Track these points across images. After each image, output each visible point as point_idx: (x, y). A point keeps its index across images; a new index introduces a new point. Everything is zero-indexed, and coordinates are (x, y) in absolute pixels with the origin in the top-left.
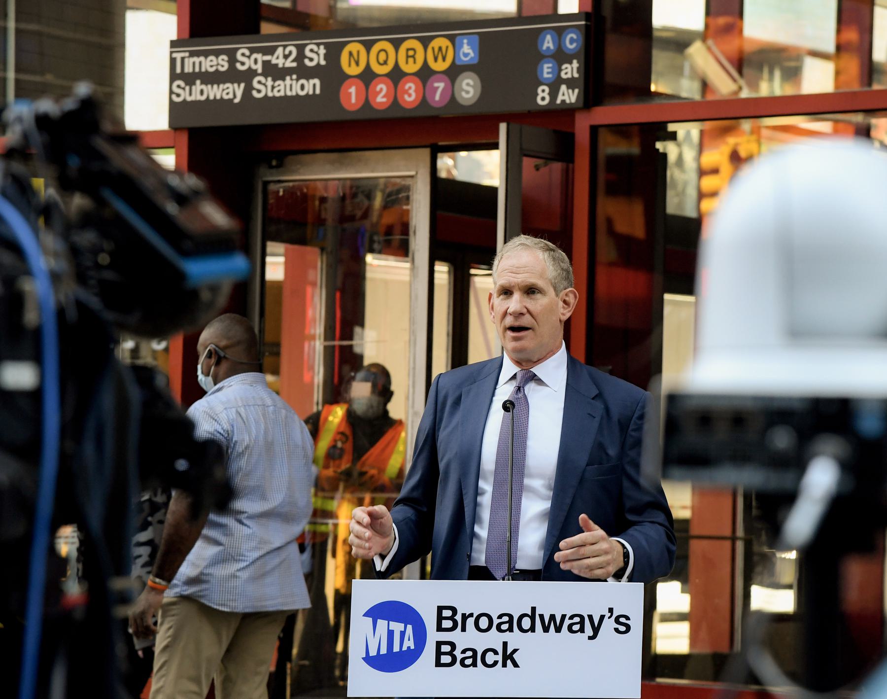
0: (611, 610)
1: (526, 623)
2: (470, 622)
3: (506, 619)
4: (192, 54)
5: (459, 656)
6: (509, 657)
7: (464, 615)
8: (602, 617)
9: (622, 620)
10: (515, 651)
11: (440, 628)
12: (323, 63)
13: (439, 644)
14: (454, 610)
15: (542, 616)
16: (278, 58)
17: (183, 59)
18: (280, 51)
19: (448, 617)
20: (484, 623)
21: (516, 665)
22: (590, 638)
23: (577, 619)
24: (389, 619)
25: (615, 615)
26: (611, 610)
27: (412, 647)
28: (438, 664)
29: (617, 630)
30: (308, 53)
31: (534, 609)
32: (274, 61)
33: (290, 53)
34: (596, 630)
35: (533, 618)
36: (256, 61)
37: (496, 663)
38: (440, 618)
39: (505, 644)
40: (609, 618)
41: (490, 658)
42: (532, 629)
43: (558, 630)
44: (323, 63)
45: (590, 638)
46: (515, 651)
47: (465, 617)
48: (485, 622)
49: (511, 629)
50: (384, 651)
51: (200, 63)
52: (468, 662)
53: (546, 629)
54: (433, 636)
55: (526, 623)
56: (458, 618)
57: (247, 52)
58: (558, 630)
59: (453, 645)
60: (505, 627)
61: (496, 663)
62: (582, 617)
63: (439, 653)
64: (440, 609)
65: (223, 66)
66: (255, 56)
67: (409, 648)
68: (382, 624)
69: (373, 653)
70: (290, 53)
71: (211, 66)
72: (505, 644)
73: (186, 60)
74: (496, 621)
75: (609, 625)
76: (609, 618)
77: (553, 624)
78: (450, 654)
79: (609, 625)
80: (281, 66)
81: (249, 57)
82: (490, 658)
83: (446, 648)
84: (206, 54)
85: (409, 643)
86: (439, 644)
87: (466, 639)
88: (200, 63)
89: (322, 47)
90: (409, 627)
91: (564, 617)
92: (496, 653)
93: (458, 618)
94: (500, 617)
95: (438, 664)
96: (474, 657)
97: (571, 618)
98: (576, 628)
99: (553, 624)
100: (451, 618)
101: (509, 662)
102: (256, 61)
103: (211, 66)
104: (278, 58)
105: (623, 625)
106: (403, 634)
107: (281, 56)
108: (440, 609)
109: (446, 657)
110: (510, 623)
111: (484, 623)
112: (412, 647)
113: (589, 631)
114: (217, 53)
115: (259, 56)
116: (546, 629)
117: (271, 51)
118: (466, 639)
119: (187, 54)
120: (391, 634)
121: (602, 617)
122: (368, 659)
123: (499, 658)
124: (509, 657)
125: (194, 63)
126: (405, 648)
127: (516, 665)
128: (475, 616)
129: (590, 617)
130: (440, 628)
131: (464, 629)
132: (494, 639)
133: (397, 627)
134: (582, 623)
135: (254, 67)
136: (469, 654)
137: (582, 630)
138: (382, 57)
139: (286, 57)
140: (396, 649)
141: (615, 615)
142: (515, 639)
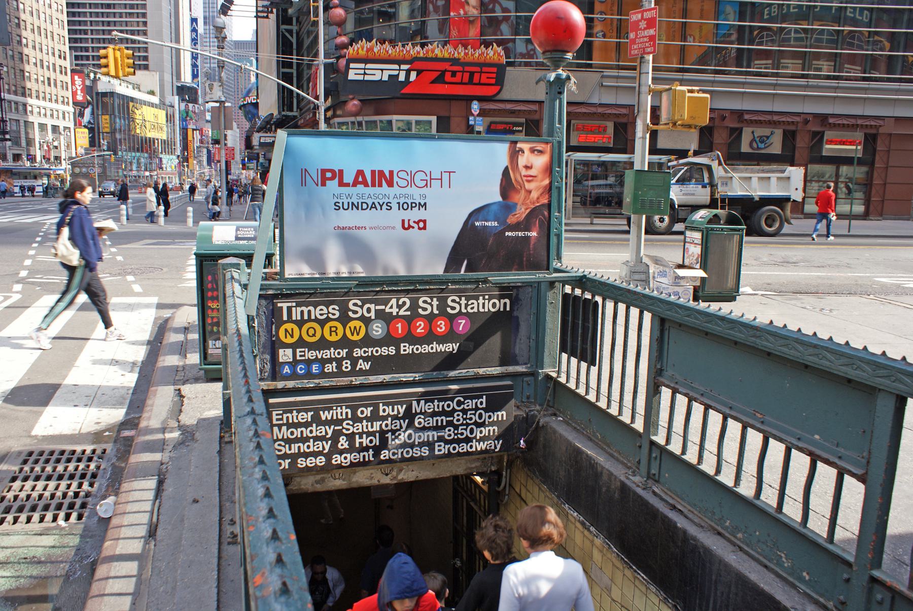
4: (299, 305)
16: (391, 307)
17: (289, 309)
18: (394, 301)
32: (388, 310)
33: (404, 303)
36: (369, 310)
51: (309, 312)
57: (360, 303)
70: (404, 303)
71: (321, 315)
73: (294, 309)
80: (395, 314)
81: (362, 307)
88: (309, 312)
102: (369, 310)
103: (321, 315)
104: (391, 307)
107: (395, 306)
115: (372, 306)
119: (294, 304)
125: (302, 312)
138: (311, 332)
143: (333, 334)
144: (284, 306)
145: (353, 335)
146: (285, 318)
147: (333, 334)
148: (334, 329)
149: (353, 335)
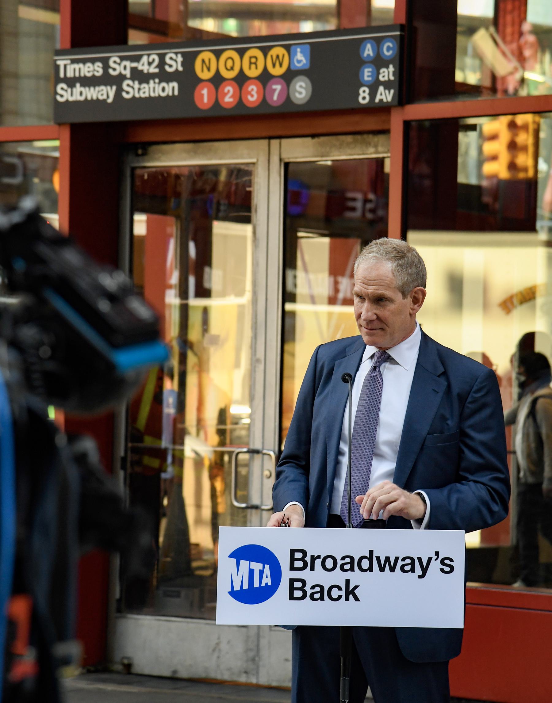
0: (437, 554)
1: (365, 564)
2: (318, 562)
3: (348, 560)
4: (73, 61)
5: (309, 592)
6: (351, 592)
7: (312, 557)
8: (430, 559)
9: (447, 562)
10: (356, 587)
11: (292, 568)
12: (180, 69)
13: (292, 581)
14: (304, 553)
15: (378, 558)
16: (143, 65)
17: (65, 66)
18: (145, 59)
19: (300, 558)
20: (329, 563)
21: (357, 599)
22: (420, 577)
23: (408, 561)
24: (250, 559)
25: (440, 558)
26: (437, 554)
27: (270, 584)
28: (292, 598)
29: (442, 570)
30: (168, 60)
31: (371, 552)
32: (140, 68)
33: (154, 60)
34: (425, 570)
35: (371, 559)
36: (125, 68)
37: (340, 597)
38: (293, 560)
39: (348, 582)
40: (436, 560)
41: (335, 593)
42: (371, 569)
43: (392, 570)
44: (180, 69)
45: (420, 577)
46: (356, 587)
47: (313, 559)
48: (330, 563)
49: (352, 569)
50: (246, 586)
51: (80, 69)
52: (317, 596)
53: (382, 569)
54: (287, 574)
55: (365, 564)
56: (308, 559)
57: (118, 60)
58: (392, 570)
59: (304, 582)
60: (347, 567)
61: (340, 597)
62: (412, 559)
63: (292, 589)
64: (293, 552)
65: (98, 72)
66: (125, 63)
67: (267, 584)
68: (244, 564)
69: (237, 588)
70: (154, 60)
71: (89, 72)
72: (348, 582)
73: (68, 67)
74: (340, 562)
75: (435, 566)
76: (436, 560)
77: (388, 565)
78: (302, 589)
79: (435, 566)
80: (145, 71)
81: (119, 64)
82: (335, 593)
83: (298, 585)
84: (84, 61)
85: (267, 580)
86: (292, 581)
87: (315, 577)
88: (80, 69)
89: (179, 56)
90: (267, 567)
91: (397, 559)
92: (340, 589)
93: (308, 559)
94: (343, 558)
95: (292, 598)
96: (322, 592)
97: (403, 560)
98: (408, 568)
99: (388, 565)
100: (302, 559)
101: (351, 597)
102: (125, 68)
103: (89, 72)
104: (143, 65)
105: (447, 566)
106: (261, 572)
107: (146, 63)
108: (293, 552)
109: (298, 591)
110: (351, 563)
111: (329, 563)
112: (270, 584)
113: (418, 570)
114: (93, 61)
115: (128, 63)
116: (382, 569)
117: (137, 59)
118: (315, 577)
119: (69, 62)
120: (251, 572)
121: (430, 559)
122: (233, 594)
123: (343, 593)
124: (351, 592)
125: (74, 70)
126: (263, 584)
127: (357, 599)
128: (322, 558)
129: (420, 559)
130: (292, 568)
131: (312, 569)
132: (338, 577)
133: (257, 566)
134: (412, 564)
135: (124, 72)
136: (317, 589)
137: (413, 570)
139: (150, 64)
140: (256, 585)
141: (440, 558)
142: (356, 577)
143: (253, 66)
144: (61, 63)
145: (274, 65)
146: (62, 75)
147: (253, 66)
148: (253, 60)
149: (274, 65)
